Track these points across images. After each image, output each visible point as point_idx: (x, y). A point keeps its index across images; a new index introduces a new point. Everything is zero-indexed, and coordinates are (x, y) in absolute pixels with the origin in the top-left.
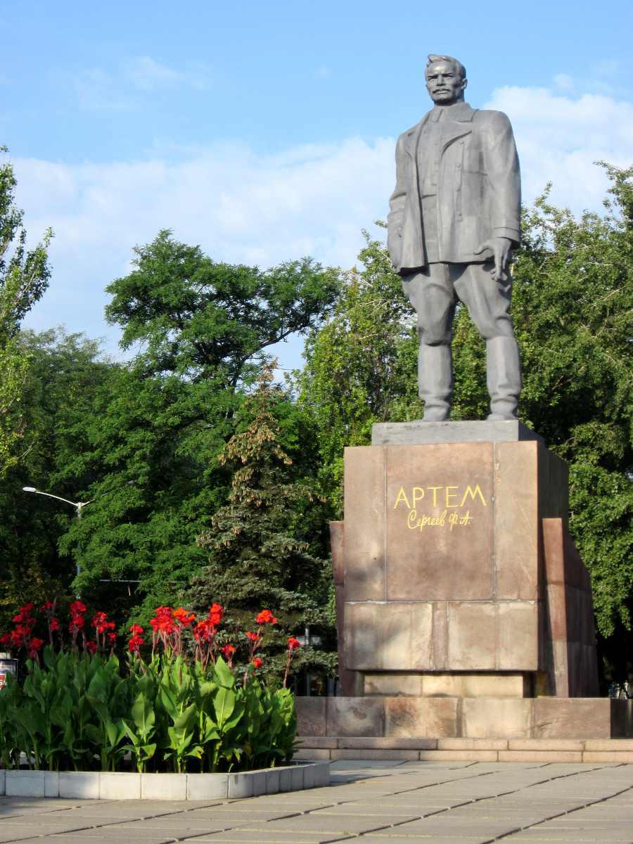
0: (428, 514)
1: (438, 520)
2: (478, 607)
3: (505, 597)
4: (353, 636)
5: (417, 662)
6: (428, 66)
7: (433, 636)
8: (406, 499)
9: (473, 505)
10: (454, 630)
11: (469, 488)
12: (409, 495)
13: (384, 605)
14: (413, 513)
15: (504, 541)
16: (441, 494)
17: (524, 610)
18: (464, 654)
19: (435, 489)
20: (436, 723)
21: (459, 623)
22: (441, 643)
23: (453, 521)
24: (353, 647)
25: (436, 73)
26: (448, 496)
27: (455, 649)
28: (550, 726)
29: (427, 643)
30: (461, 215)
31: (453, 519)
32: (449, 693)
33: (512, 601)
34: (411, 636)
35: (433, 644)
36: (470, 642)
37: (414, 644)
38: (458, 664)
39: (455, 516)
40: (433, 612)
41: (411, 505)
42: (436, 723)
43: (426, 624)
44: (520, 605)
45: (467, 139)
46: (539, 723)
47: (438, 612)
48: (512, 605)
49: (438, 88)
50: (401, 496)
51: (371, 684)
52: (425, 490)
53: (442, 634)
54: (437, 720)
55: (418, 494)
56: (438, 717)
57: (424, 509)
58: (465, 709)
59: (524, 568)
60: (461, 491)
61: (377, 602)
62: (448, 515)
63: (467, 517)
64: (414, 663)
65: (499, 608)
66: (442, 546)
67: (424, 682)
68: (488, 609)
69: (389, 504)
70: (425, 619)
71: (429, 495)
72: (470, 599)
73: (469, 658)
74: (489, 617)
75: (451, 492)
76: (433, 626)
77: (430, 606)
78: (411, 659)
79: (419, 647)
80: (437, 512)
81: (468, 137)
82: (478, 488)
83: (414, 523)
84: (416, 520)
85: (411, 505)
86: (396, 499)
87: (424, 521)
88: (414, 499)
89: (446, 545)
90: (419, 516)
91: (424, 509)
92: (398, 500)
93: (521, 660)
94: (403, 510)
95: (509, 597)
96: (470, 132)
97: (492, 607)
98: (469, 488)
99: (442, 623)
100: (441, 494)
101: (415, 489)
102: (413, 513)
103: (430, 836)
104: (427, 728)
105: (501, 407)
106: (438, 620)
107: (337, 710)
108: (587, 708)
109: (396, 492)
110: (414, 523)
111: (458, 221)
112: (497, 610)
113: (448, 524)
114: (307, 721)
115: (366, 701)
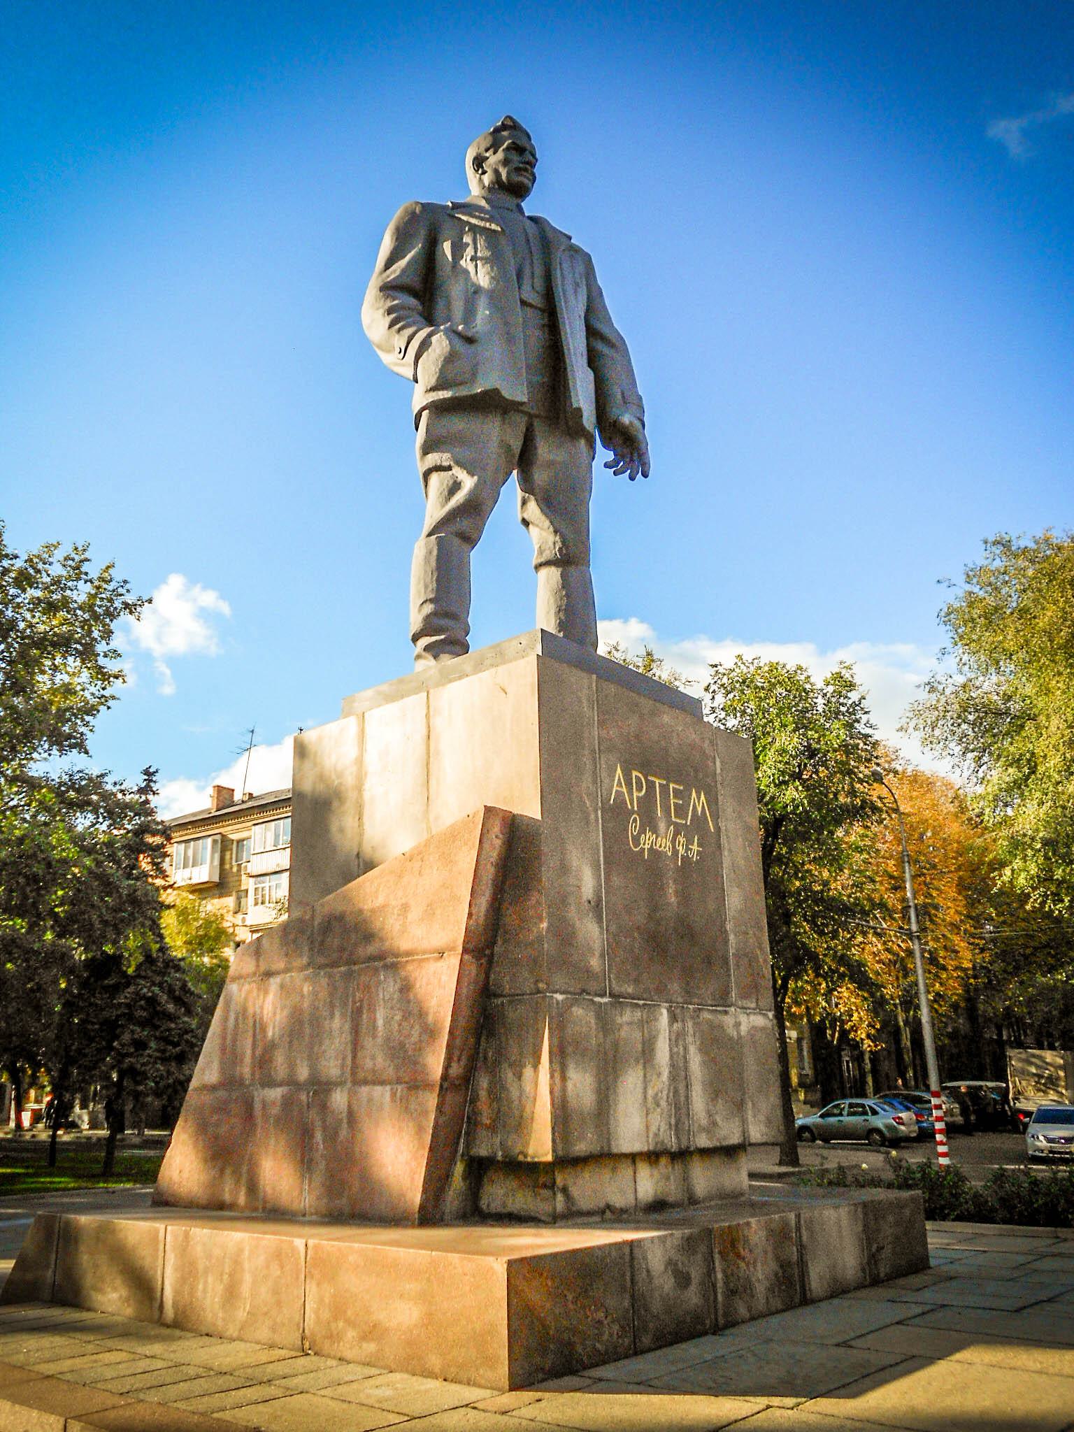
1: (664, 844)
5: (656, 1135)
8: (624, 790)
11: (694, 795)
13: (606, 1004)
18: (710, 1114)
21: (700, 1050)
29: (665, 1093)
32: (671, 1199)
37: (650, 1092)
42: (776, 1275)
47: (675, 1025)
61: (597, 999)
64: (651, 1135)
71: (651, 786)
72: (710, 1002)
73: (714, 1124)
77: (665, 1012)
80: (662, 826)
84: (639, 834)
87: (647, 840)
89: (676, 892)
90: (642, 831)
93: (769, 1121)
102: (635, 819)
113: (675, 852)
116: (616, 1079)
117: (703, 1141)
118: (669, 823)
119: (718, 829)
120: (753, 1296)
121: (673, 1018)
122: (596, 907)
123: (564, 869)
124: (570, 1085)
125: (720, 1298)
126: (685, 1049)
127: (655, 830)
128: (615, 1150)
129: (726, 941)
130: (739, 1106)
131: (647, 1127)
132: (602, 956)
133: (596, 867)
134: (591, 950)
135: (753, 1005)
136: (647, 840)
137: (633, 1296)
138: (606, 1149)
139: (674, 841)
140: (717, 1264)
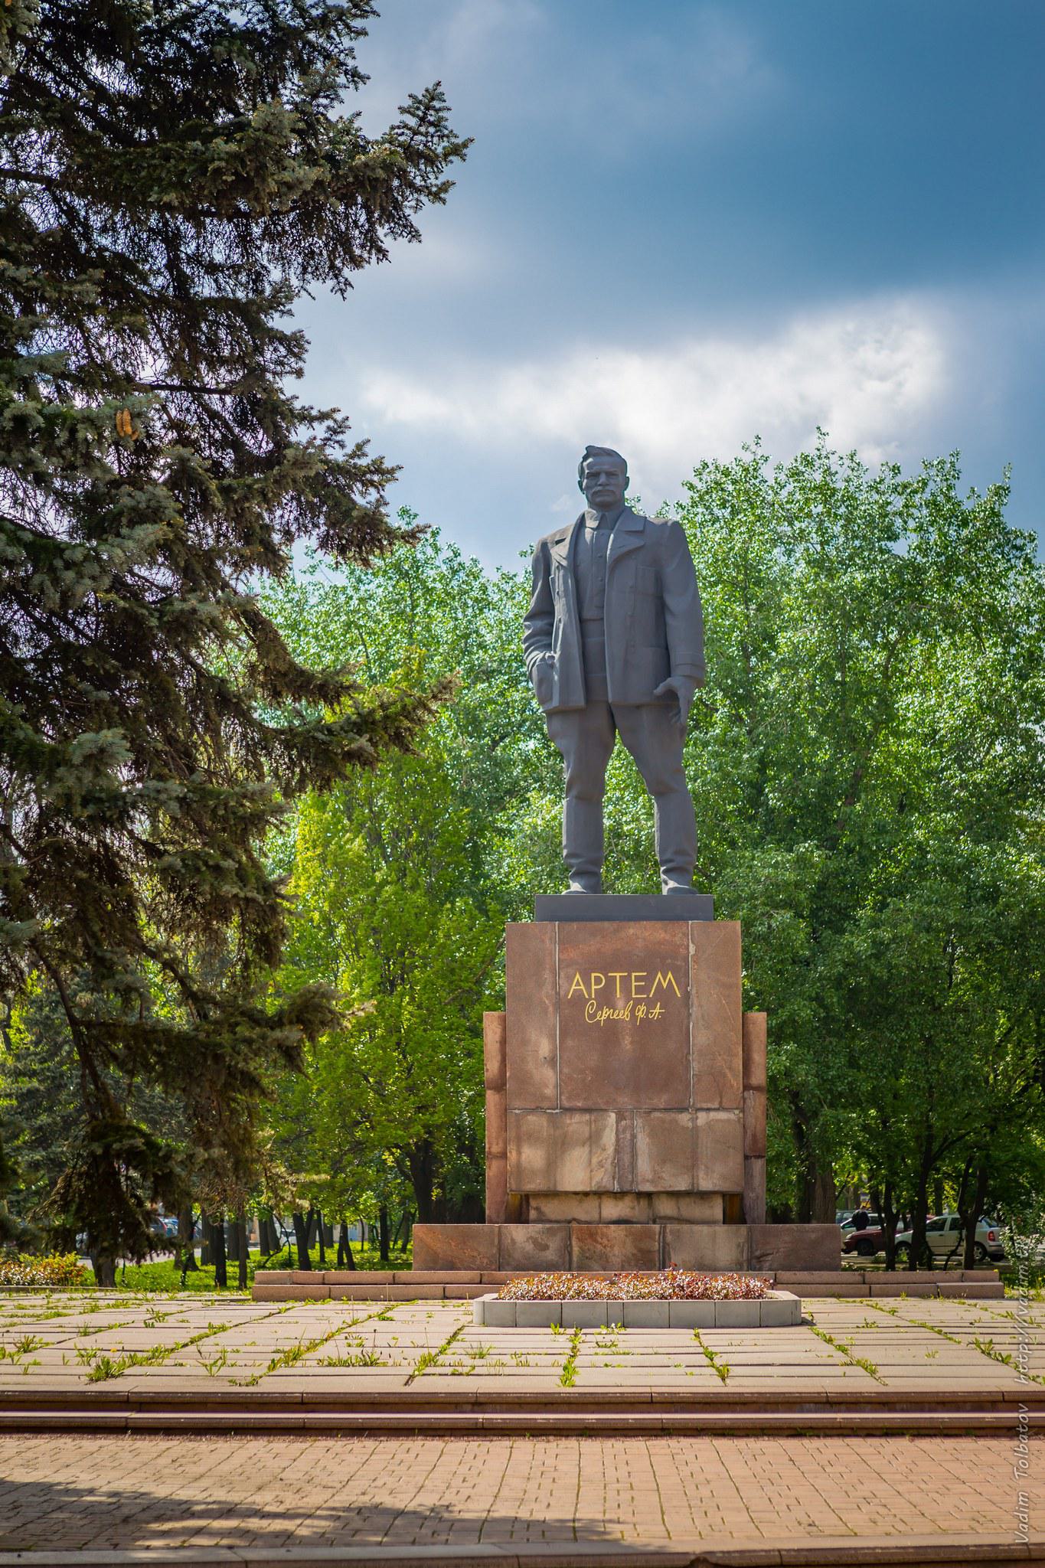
0: (612, 1006)
1: (622, 1014)
2: (672, 1115)
3: (705, 1106)
4: (519, 1153)
7: (617, 1151)
8: (582, 987)
9: (665, 996)
10: (643, 1142)
11: (659, 975)
12: (588, 984)
14: (592, 1004)
15: (700, 1038)
16: (625, 981)
17: (728, 1121)
19: (618, 975)
20: (633, 1255)
22: (627, 1158)
23: (640, 1015)
24: (519, 1165)
26: (634, 984)
27: (644, 1166)
28: (770, 1258)
29: (609, 1161)
33: (709, 1110)
34: (590, 1151)
35: (617, 1163)
36: (664, 1157)
37: (595, 1160)
38: (648, 1184)
39: (643, 1008)
40: (617, 1123)
41: (590, 994)
42: (633, 1255)
43: (609, 1138)
44: (722, 1115)
46: (758, 1253)
47: (623, 1123)
48: (713, 1115)
50: (577, 984)
51: (537, 1209)
53: (628, 1149)
54: (635, 1251)
55: (598, 981)
56: (635, 1247)
57: (606, 998)
58: (669, 1238)
59: (727, 1071)
60: (649, 979)
63: (657, 1010)
65: (697, 1118)
66: (627, 1042)
67: (603, 1206)
68: (684, 1119)
69: (562, 993)
70: (608, 1130)
71: (611, 981)
74: (686, 1128)
75: (638, 979)
76: (618, 1140)
77: (613, 1115)
78: (591, 1178)
79: (601, 1165)
80: (620, 1004)
82: (670, 975)
83: (592, 1016)
85: (590, 994)
87: (605, 1014)
88: (594, 987)
89: (632, 1043)
90: (600, 1008)
91: (606, 998)
92: (573, 987)
94: (579, 1001)
95: (709, 1105)
97: (689, 1116)
98: (659, 975)
99: (628, 1136)
100: (625, 981)
101: (593, 975)
102: (592, 1004)
103: (940, 1284)
104: (622, 1261)
105: (35, 414)
106: (624, 1131)
107: (513, 1240)
108: (813, 1236)
109: (570, 979)
110: (592, 1016)
112: (694, 1120)
114: (475, 1254)
115: (548, 1229)
116: (563, 1152)
117: (648, 1187)
118: (628, 998)
119: (687, 995)
120: (607, 1262)
121: (620, 1117)
122: (552, 1061)
123: (524, 1042)
124: (524, 1156)
125: (575, 1259)
126: (634, 1136)
127: (612, 1006)
128: (560, 1188)
129: (687, 1068)
130: (692, 1168)
131: (591, 1178)
132: (556, 1086)
133: (552, 1037)
134: (547, 1086)
135: (716, 1106)
136: (605, 1014)
137: (499, 1249)
138: (552, 1188)
139: (632, 1012)
140: (574, 1243)
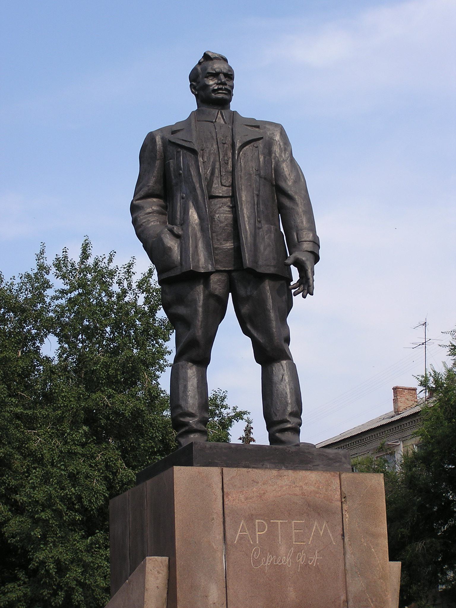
6: (200, 63)
25: (217, 70)
30: (260, 222)
31: (301, 559)
45: (260, 144)
49: (220, 87)
52: (269, 523)
62: (295, 553)
80: (282, 549)
81: (260, 141)
83: (257, 562)
85: (254, 539)
86: (236, 533)
87: (269, 559)
96: (262, 138)
102: (256, 550)
111: (259, 228)
136: (269, 559)
